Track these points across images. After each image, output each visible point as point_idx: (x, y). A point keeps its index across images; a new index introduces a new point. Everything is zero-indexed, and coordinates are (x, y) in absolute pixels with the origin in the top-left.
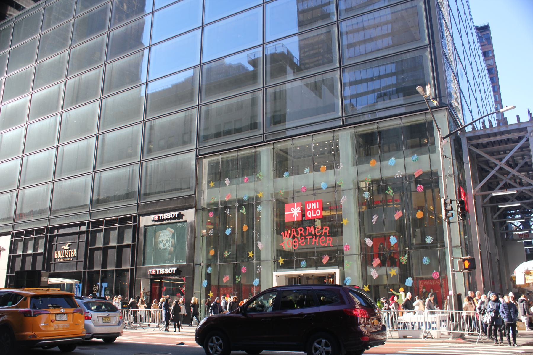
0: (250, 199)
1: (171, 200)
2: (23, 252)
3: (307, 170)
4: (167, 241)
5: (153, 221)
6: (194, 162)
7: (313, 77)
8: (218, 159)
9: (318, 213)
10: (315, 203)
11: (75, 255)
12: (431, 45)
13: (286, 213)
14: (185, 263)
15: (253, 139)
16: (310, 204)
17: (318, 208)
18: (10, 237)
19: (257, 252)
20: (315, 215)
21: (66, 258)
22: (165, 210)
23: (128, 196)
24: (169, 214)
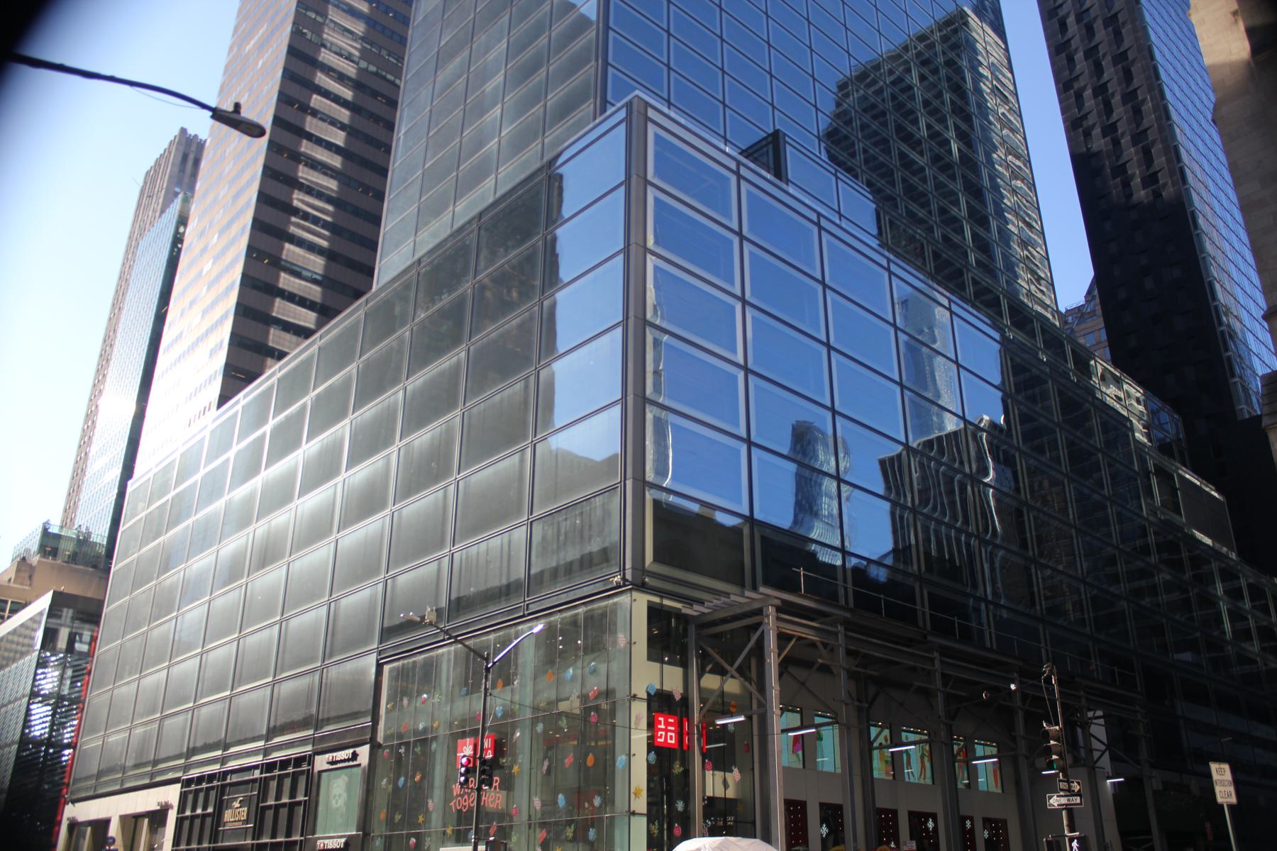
0: (425, 730)
2: (192, 812)
4: (340, 795)
5: (328, 763)
6: (373, 670)
11: (245, 818)
14: (354, 833)
18: (179, 785)
19: (427, 813)
21: (235, 821)
24: (343, 752)
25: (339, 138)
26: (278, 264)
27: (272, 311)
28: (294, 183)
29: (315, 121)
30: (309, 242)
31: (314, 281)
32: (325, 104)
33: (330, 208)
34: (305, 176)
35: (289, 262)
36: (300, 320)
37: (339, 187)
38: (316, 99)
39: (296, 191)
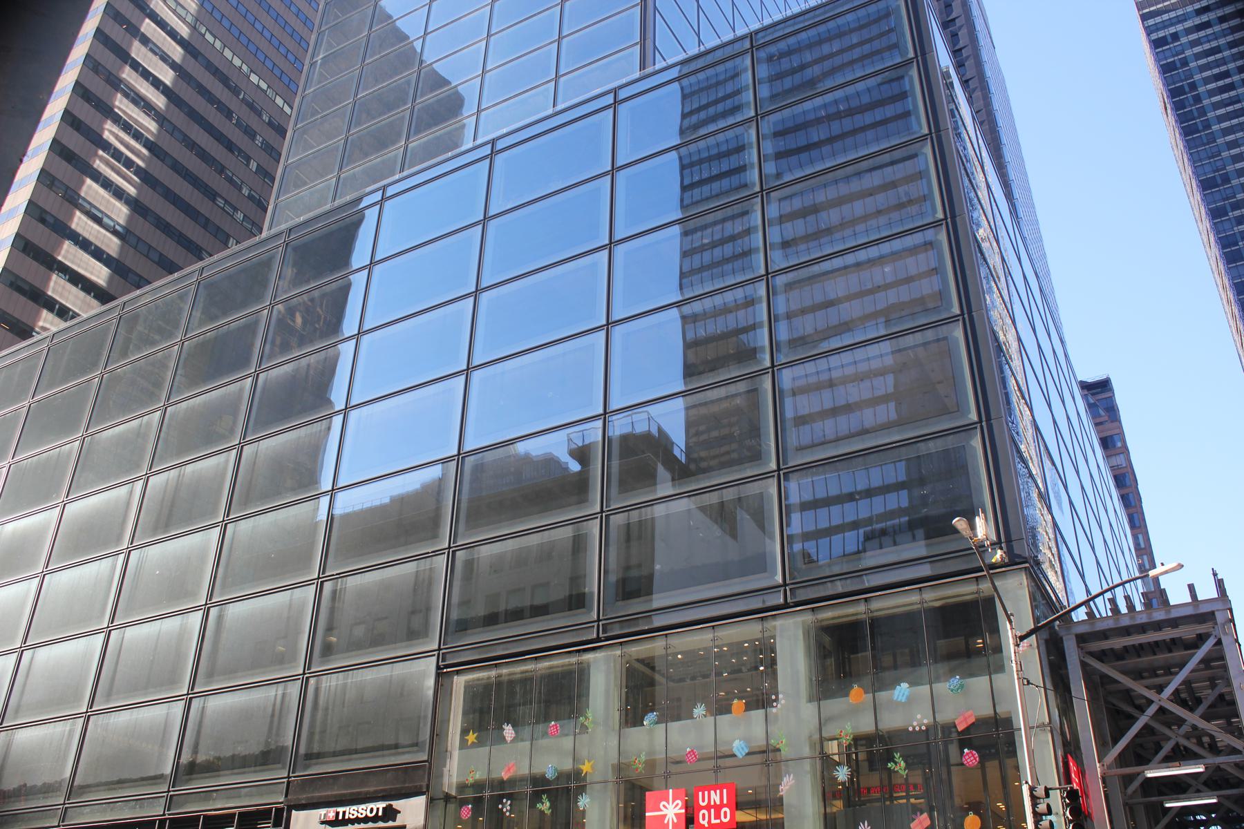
1: (370, 773)
3: (699, 711)
6: (430, 682)
7: (716, 493)
8: (489, 678)
9: (725, 817)
10: (718, 791)
12: (984, 424)
13: (647, 814)
15: (574, 633)
16: (706, 793)
17: (725, 802)
20: (718, 821)
22: (353, 797)
23: (267, 758)
24: (364, 806)
25: (167, 76)
26: (73, 200)
27: (59, 254)
28: (108, 112)
29: (143, 49)
30: (117, 185)
31: (115, 232)
32: (160, 34)
33: (145, 151)
34: (122, 107)
35: (90, 203)
36: (92, 273)
37: (159, 132)
38: (148, 24)
39: (109, 122)
